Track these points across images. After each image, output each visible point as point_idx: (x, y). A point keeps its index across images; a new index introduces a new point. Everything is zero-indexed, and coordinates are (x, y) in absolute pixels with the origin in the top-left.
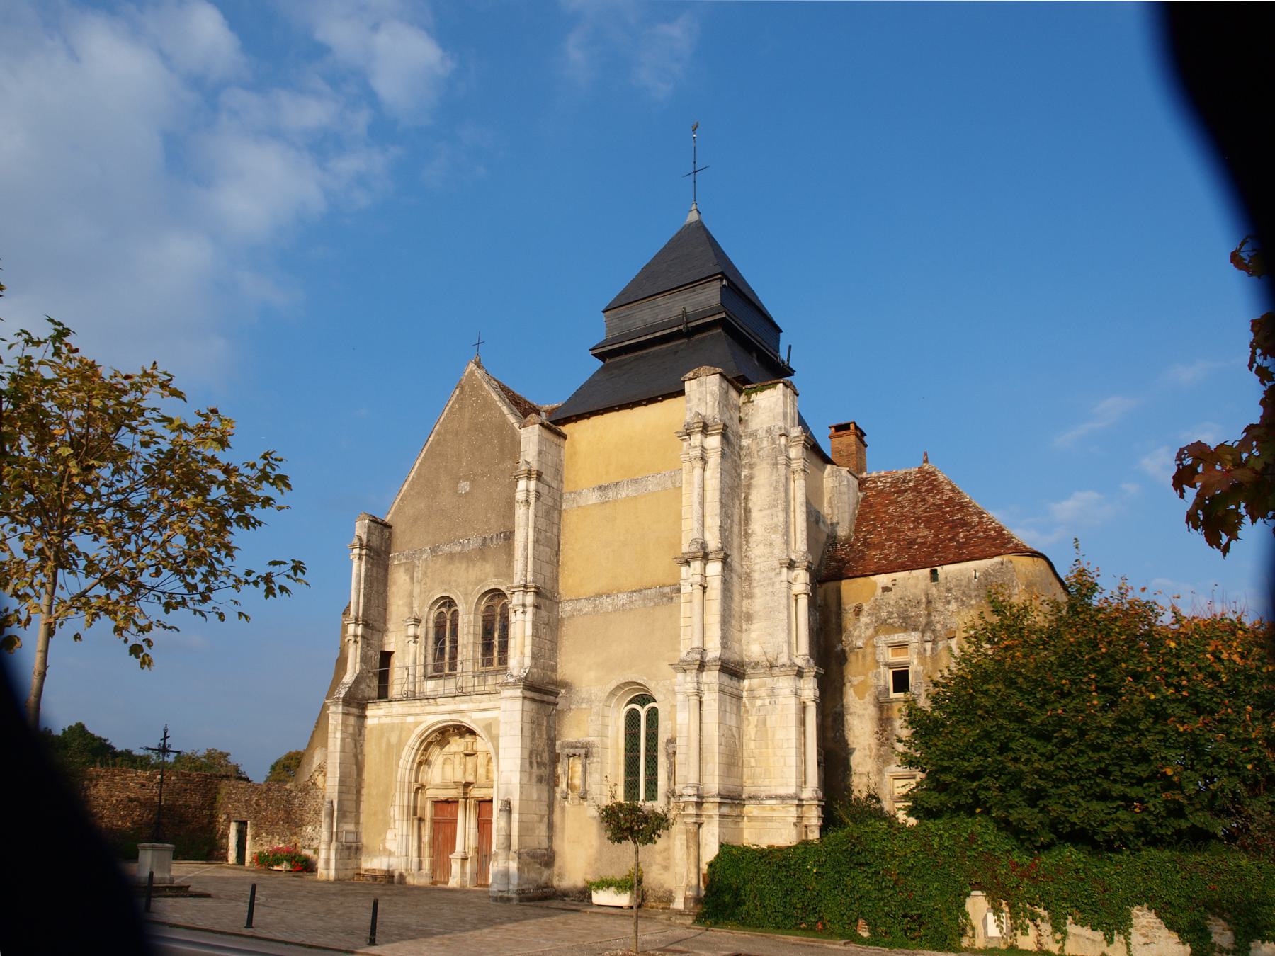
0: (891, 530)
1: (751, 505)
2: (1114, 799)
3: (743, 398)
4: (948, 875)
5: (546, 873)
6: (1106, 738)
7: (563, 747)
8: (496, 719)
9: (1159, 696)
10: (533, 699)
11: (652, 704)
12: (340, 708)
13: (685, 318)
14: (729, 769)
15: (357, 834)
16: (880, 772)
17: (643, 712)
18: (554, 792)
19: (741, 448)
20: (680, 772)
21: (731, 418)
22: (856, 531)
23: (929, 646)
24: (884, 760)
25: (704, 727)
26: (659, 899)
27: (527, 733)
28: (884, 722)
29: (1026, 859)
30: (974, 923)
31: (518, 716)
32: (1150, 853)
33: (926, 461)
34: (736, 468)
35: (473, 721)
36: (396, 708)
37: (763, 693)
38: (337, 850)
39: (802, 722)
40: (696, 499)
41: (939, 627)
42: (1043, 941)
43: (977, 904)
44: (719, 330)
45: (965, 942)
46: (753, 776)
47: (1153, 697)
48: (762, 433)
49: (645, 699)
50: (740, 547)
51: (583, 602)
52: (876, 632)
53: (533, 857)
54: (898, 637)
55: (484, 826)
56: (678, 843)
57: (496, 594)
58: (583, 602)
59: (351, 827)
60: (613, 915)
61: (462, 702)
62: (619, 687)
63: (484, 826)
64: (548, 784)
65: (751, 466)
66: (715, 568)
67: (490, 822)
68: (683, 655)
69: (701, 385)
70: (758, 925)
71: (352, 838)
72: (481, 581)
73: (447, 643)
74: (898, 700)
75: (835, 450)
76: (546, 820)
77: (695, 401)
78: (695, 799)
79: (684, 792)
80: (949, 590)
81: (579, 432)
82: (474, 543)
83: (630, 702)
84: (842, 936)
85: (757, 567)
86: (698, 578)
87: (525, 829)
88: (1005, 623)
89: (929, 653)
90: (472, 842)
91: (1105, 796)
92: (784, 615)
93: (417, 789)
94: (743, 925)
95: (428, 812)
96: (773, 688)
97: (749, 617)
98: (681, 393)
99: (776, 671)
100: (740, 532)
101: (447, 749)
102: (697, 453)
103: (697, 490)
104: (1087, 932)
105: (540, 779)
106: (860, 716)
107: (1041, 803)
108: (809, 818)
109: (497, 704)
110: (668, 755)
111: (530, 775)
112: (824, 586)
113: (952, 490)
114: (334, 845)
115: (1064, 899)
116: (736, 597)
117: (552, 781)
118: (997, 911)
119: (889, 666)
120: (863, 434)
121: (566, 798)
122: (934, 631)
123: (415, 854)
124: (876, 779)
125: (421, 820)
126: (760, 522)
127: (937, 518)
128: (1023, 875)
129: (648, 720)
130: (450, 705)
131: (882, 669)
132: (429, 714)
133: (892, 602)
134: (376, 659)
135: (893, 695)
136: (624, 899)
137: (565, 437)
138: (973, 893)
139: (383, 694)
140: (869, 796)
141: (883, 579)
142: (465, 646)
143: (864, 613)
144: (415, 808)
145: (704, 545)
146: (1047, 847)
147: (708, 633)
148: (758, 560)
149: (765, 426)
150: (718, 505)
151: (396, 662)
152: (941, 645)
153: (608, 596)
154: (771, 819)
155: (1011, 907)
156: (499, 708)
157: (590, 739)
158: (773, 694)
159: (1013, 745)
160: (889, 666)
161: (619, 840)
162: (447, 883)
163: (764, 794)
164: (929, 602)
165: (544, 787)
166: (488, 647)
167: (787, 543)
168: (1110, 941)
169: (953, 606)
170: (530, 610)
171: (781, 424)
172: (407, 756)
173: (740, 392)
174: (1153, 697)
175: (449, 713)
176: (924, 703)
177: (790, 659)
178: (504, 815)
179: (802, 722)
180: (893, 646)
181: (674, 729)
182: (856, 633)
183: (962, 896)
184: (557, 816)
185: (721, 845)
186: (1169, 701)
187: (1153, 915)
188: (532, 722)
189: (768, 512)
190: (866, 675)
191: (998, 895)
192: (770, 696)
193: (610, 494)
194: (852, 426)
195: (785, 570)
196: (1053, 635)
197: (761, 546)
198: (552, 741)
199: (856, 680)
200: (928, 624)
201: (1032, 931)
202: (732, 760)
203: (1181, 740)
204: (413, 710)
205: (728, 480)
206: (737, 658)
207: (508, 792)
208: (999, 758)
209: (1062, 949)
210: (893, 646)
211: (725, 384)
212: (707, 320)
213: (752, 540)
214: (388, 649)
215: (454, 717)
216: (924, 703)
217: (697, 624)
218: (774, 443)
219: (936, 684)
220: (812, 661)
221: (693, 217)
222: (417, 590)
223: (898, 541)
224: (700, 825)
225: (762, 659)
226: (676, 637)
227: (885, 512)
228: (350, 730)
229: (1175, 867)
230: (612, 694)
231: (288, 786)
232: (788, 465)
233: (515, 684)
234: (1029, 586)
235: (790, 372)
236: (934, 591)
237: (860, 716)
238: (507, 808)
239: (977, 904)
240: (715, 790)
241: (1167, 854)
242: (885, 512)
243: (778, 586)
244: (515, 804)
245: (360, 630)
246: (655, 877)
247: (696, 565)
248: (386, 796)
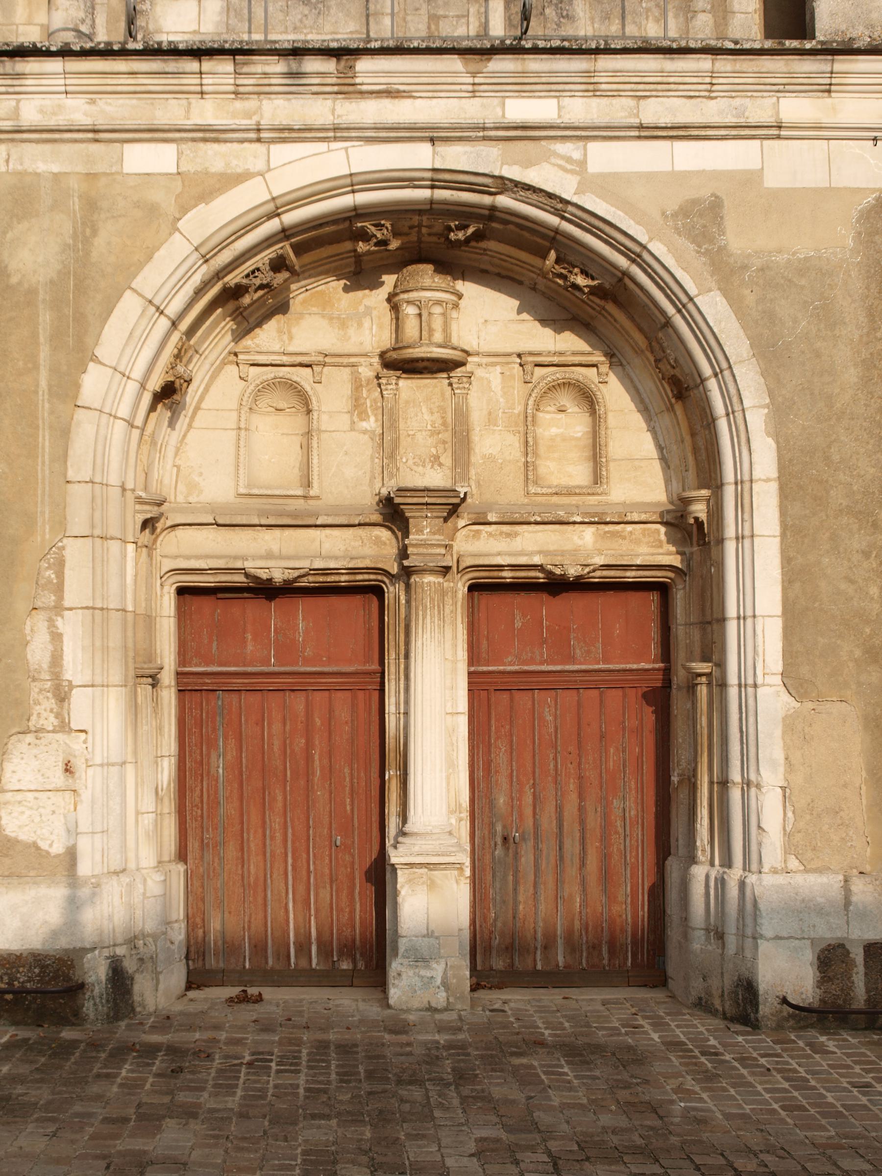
35: (606, 184)
61: (524, 87)
101: (268, 338)
130: (442, 96)
132: (288, 134)
172: (128, 344)
175: (434, 135)
204: (171, 112)
215: (458, 157)
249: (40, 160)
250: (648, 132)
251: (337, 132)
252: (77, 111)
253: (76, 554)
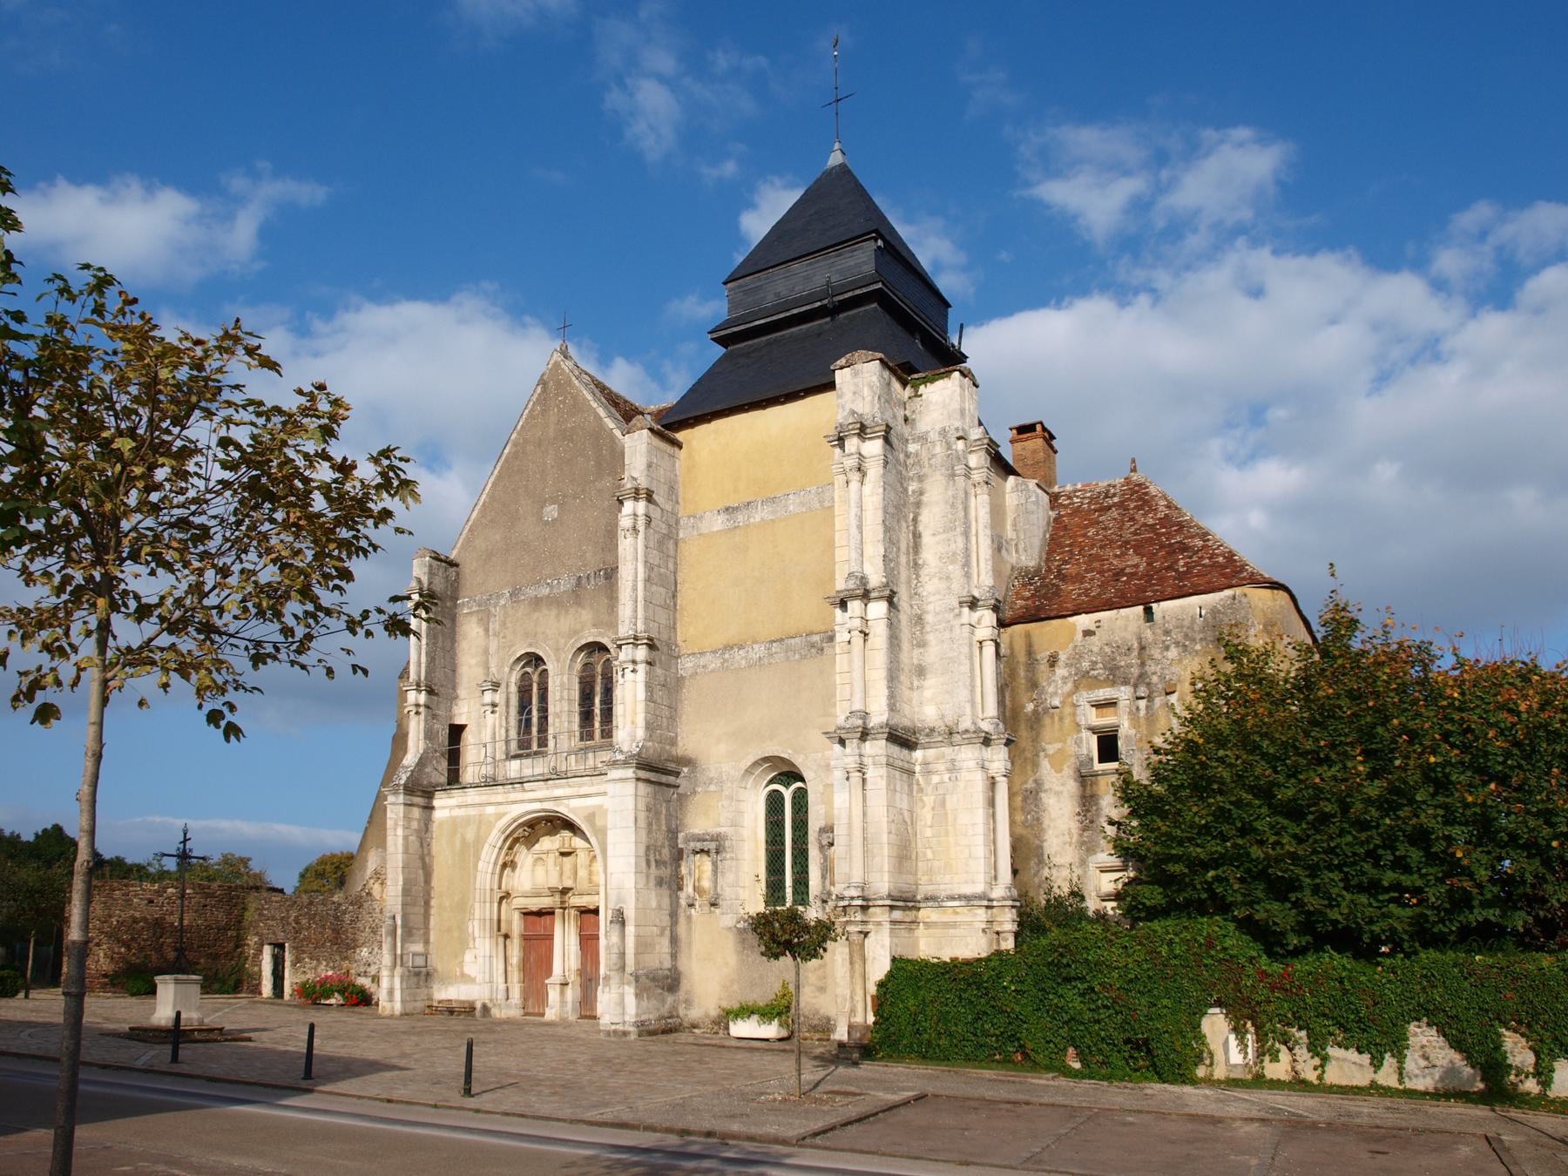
0: (1093, 558)
1: (921, 528)
2: (1387, 890)
3: (909, 391)
4: (1180, 989)
5: (670, 999)
6: (1374, 812)
7: (687, 840)
8: (601, 806)
9: (1440, 760)
10: (648, 781)
11: (799, 784)
12: (401, 798)
13: (829, 290)
14: (900, 863)
15: (426, 955)
16: (1083, 863)
17: (787, 794)
18: (678, 898)
19: (907, 456)
20: (840, 869)
21: (895, 417)
22: (1047, 560)
24: (1088, 848)
25: (869, 811)
26: (814, 1028)
27: (642, 824)
28: (1088, 801)
29: (1277, 967)
30: (1212, 1047)
31: (630, 803)
32: (1428, 956)
33: (1134, 470)
34: (902, 480)
35: (573, 810)
36: (472, 796)
37: (942, 767)
38: (402, 977)
39: (992, 803)
40: (854, 522)
41: (1155, 679)
42: (1299, 1068)
43: (1215, 1025)
44: (874, 305)
45: (1201, 1072)
46: (930, 872)
47: (1432, 759)
48: (933, 436)
49: (790, 774)
50: (909, 582)
51: (709, 657)
52: (1077, 687)
53: (654, 979)
54: (1103, 693)
55: (588, 942)
56: (838, 958)
57: (596, 648)
58: (709, 657)
59: (418, 947)
60: (758, 1049)
61: (556, 787)
62: (756, 764)
63: (588, 942)
64: (670, 887)
65: (921, 479)
66: (878, 609)
67: (597, 938)
68: (841, 720)
69: (856, 374)
70: (944, 1058)
71: (420, 961)
72: (576, 632)
73: (535, 713)
74: (1105, 773)
75: (1017, 457)
76: (668, 933)
77: (848, 396)
78: (859, 902)
79: (847, 894)
80: (1167, 633)
81: (701, 439)
82: (566, 584)
83: (771, 782)
84: (1049, 1068)
85: (930, 608)
86: (857, 623)
87: (643, 946)
88: (1242, 675)
89: (1142, 713)
90: (574, 961)
91: (1373, 888)
92: (966, 668)
93: (502, 899)
94: (924, 1057)
95: (516, 925)
96: (953, 760)
97: (921, 671)
98: (830, 386)
99: (957, 738)
100: (908, 562)
102: (851, 462)
103: (854, 510)
104: (1352, 1055)
105: (660, 882)
106: (1058, 793)
107: (1293, 897)
108: (1001, 923)
109: (601, 788)
110: (821, 847)
111: (648, 876)
112: (1009, 630)
113: (1168, 507)
114: (399, 970)
115: (1324, 1015)
116: (905, 646)
117: (676, 884)
118: (1239, 1031)
119: (1093, 730)
120: (1052, 437)
121: (691, 905)
122: (1148, 684)
123: (501, 979)
124: (1078, 871)
125: (506, 936)
126: (931, 552)
127: (1150, 541)
128: (1273, 989)
129: (794, 804)
130: (542, 791)
131: (1085, 734)
132: (514, 802)
133: (1096, 649)
134: (443, 735)
135: (1098, 767)
136: (771, 1030)
137: (680, 446)
138: (1211, 1011)
139: (454, 779)
140: (1073, 894)
141: (1084, 621)
142: (557, 715)
143: (1061, 663)
144: (499, 921)
145: (863, 580)
146: (1299, 952)
147: (872, 692)
148: (932, 599)
149: (938, 427)
150: (881, 529)
151: (468, 737)
152: (1158, 701)
153: (741, 647)
154: (954, 925)
155: (1258, 1027)
156: (605, 793)
157: (719, 830)
158: (953, 768)
159: (1257, 825)
160: (1093, 730)
161: (776, 957)
162: (543, 1015)
163: (943, 894)
164: (1142, 648)
165: (665, 892)
166: (586, 716)
167: (967, 575)
168: (1377, 1064)
169: (1173, 653)
170: (641, 668)
171: (958, 424)
173: (904, 384)
174: (1432, 759)
175: (540, 800)
176: (1141, 775)
177: (974, 723)
178: (617, 927)
179: (992, 803)
180: (1099, 706)
181: (829, 814)
182: (1051, 690)
183: (1198, 1012)
184: (682, 929)
185: (894, 960)
186: (1452, 765)
187: (1433, 1031)
188: (649, 810)
189: (944, 536)
190: (1064, 742)
191: (1243, 1013)
192: (950, 770)
193: (741, 518)
194: (1039, 427)
195: (966, 610)
196: (1305, 684)
197: (936, 580)
198: (673, 833)
199: (1052, 749)
200: (1142, 676)
201: (1284, 1055)
202: (904, 854)
203: (1468, 812)
204: (493, 799)
205: (892, 496)
206: (907, 723)
207: (620, 899)
208: (1240, 841)
209: (1320, 1078)
210: (1099, 706)
211: (886, 374)
212: (858, 292)
213: (923, 572)
214: (458, 721)
216: (1141, 775)
217: (859, 681)
218: (949, 448)
219: (1157, 752)
220: (1001, 726)
221: (835, 159)
222: (493, 645)
223: (1101, 572)
224: (866, 934)
225: (940, 725)
226: (829, 699)
227: (1084, 535)
228: (415, 825)
229: (1461, 972)
230: (748, 772)
231: (335, 899)
232: (967, 476)
233: (625, 763)
234: (1269, 626)
235: (963, 358)
236: (1148, 634)
237: (1058, 793)
238: (620, 919)
239: (1215, 1025)
240: (884, 891)
241: (1451, 955)
242: (1084, 535)
243: (957, 630)
244: (630, 914)
245: (422, 698)
246: (811, 1001)
247: (855, 606)
248: (463, 907)
249: (472, 812)
250: (581, 796)
251: (522, 801)
252: (478, 799)
253: (477, 906)
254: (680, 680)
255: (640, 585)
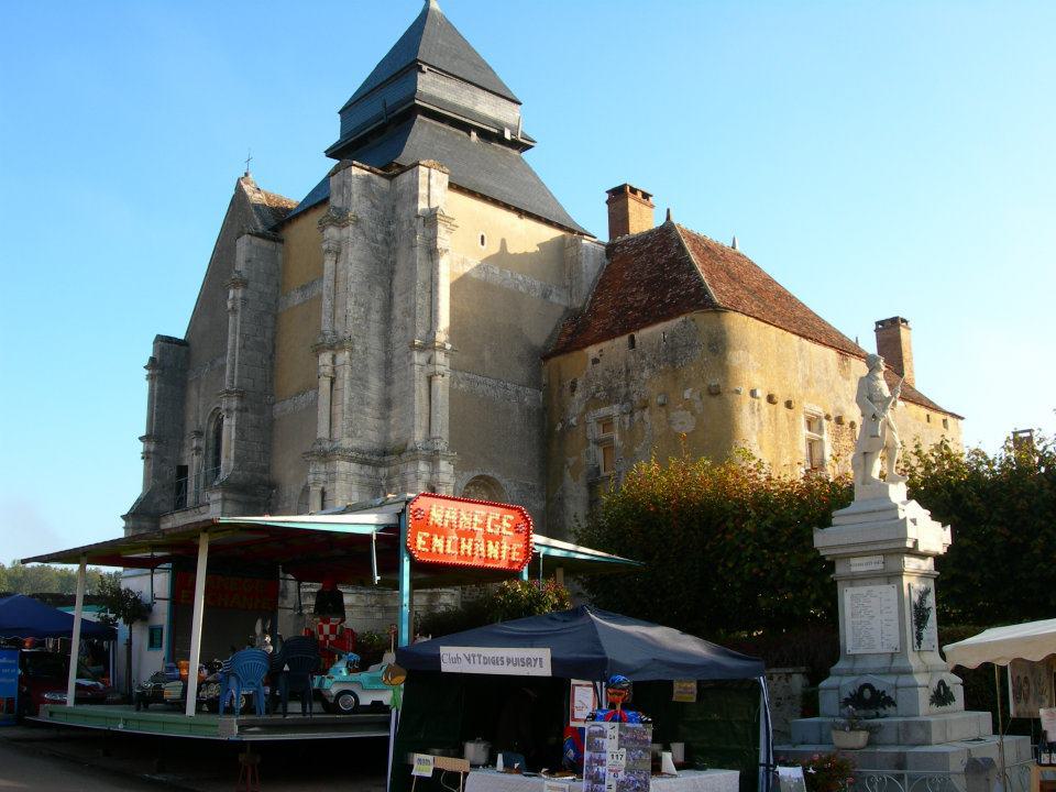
23: (627, 418)
113: (678, 248)
131: (592, 447)
134: (171, 473)
141: (592, 351)
143: (579, 388)
152: (637, 416)
164: (628, 371)
182: (571, 411)
199: (571, 461)
213: (394, 325)
214: (186, 463)
236: (632, 360)
254: (272, 422)
255: (237, 351)
